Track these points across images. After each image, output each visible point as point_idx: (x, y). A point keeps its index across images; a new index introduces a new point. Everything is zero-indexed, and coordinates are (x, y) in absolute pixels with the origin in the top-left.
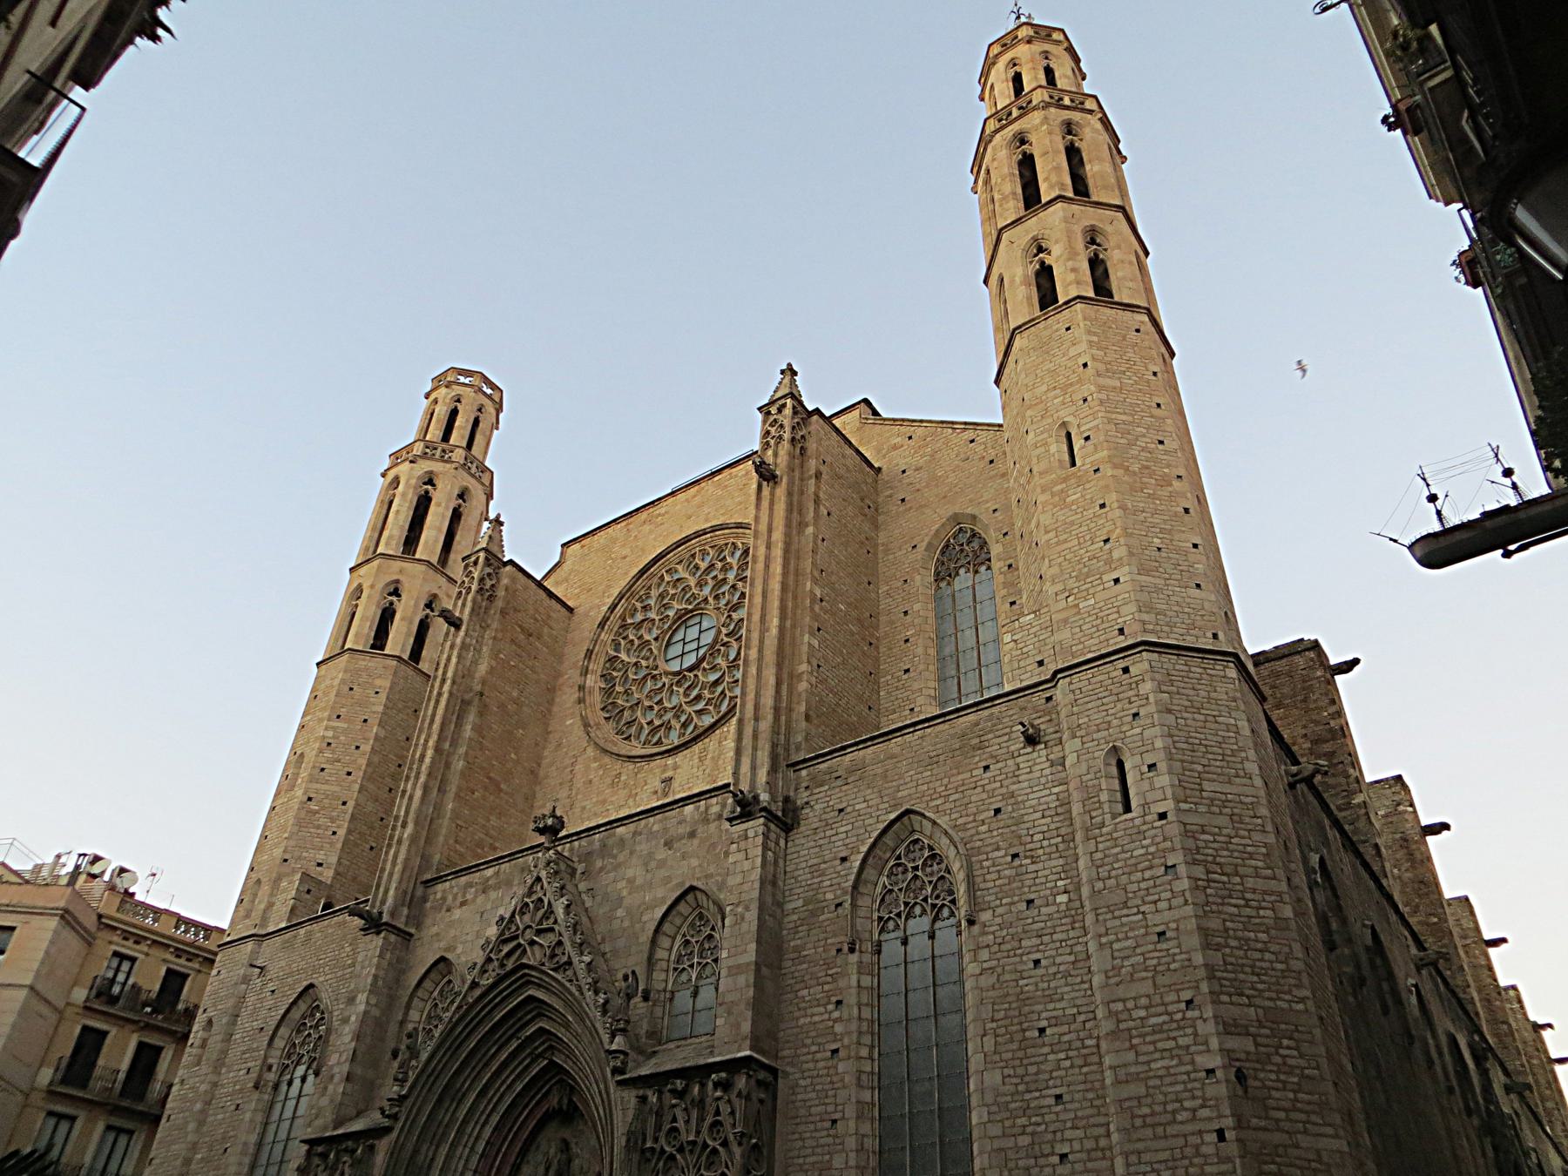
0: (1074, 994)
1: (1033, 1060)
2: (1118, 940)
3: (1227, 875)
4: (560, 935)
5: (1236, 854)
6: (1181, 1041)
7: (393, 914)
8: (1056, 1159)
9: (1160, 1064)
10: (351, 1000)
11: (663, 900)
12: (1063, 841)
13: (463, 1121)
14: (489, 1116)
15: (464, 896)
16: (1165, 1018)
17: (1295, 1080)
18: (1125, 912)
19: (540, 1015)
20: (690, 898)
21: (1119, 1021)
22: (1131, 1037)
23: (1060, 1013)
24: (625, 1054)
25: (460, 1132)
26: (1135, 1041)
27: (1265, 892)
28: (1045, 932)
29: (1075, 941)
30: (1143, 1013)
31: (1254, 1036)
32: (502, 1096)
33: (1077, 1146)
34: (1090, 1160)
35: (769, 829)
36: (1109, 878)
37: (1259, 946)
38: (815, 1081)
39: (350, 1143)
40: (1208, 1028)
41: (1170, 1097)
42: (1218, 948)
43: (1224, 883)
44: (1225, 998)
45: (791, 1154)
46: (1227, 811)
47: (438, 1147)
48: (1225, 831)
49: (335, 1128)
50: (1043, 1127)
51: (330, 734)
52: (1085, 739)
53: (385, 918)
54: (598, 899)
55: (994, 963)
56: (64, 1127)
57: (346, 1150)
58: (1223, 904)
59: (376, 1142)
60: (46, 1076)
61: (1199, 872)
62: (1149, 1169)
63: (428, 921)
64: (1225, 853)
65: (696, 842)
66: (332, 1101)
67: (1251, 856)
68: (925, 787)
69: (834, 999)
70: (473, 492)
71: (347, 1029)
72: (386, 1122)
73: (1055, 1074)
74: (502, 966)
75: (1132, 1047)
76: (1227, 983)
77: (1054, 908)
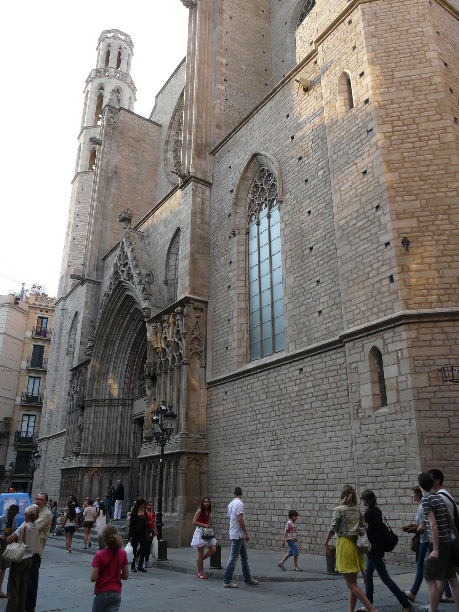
0: (326, 223)
1: (307, 265)
2: (344, 184)
3: (407, 125)
5: (415, 111)
6: (373, 232)
7: (89, 275)
8: (317, 314)
9: (362, 248)
12: (321, 140)
13: (117, 353)
14: (127, 349)
16: (365, 220)
17: (445, 237)
18: (348, 166)
21: (343, 231)
22: (348, 237)
23: (319, 236)
24: (150, 309)
26: (350, 239)
27: (433, 130)
28: (312, 194)
29: (325, 194)
30: (354, 222)
31: (417, 217)
32: (130, 339)
33: (326, 305)
34: (331, 311)
35: (197, 187)
36: (340, 150)
37: (426, 163)
38: (222, 303)
40: (386, 219)
41: (366, 265)
42: (396, 170)
43: (404, 131)
44: (399, 199)
45: (214, 340)
46: (412, 86)
47: (109, 364)
48: (408, 99)
50: (311, 299)
51: (77, 210)
52: (329, 76)
53: (86, 277)
54: (151, 246)
55: (291, 220)
56: (37, 382)
58: (403, 143)
60: (24, 365)
61: (387, 128)
62: (355, 308)
64: (407, 112)
67: (426, 110)
68: (262, 139)
69: (228, 262)
70: (123, 88)
73: (317, 269)
75: (349, 242)
76: (402, 189)
77: (317, 180)
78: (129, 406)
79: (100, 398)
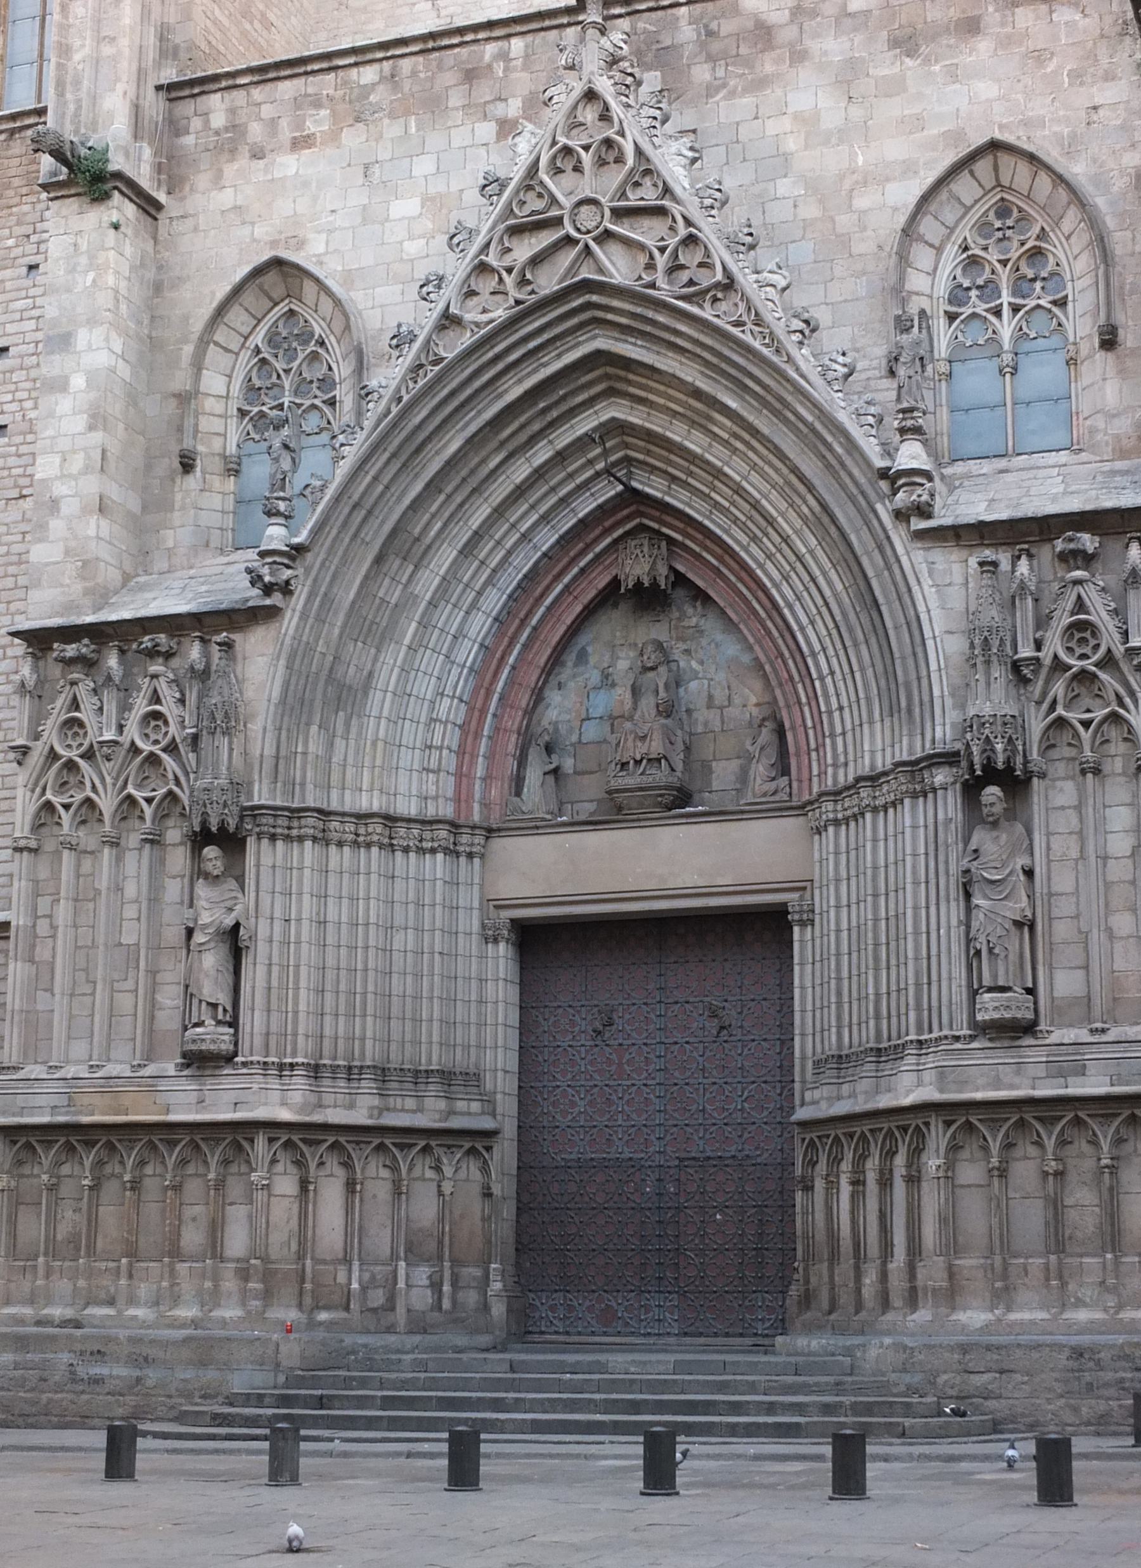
4: (688, 222)
10: (63, 341)
11: (909, 169)
15: (299, 124)
19: (611, 392)
20: (983, 167)
25: (424, 624)
39: (162, 638)
49: (97, 609)
57: (152, 653)
59: (236, 637)
63: (202, 180)
65: (984, 46)
66: (67, 552)
71: (64, 404)
72: (254, 596)
74: (523, 282)
78: (470, 856)
79: (335, 806)
